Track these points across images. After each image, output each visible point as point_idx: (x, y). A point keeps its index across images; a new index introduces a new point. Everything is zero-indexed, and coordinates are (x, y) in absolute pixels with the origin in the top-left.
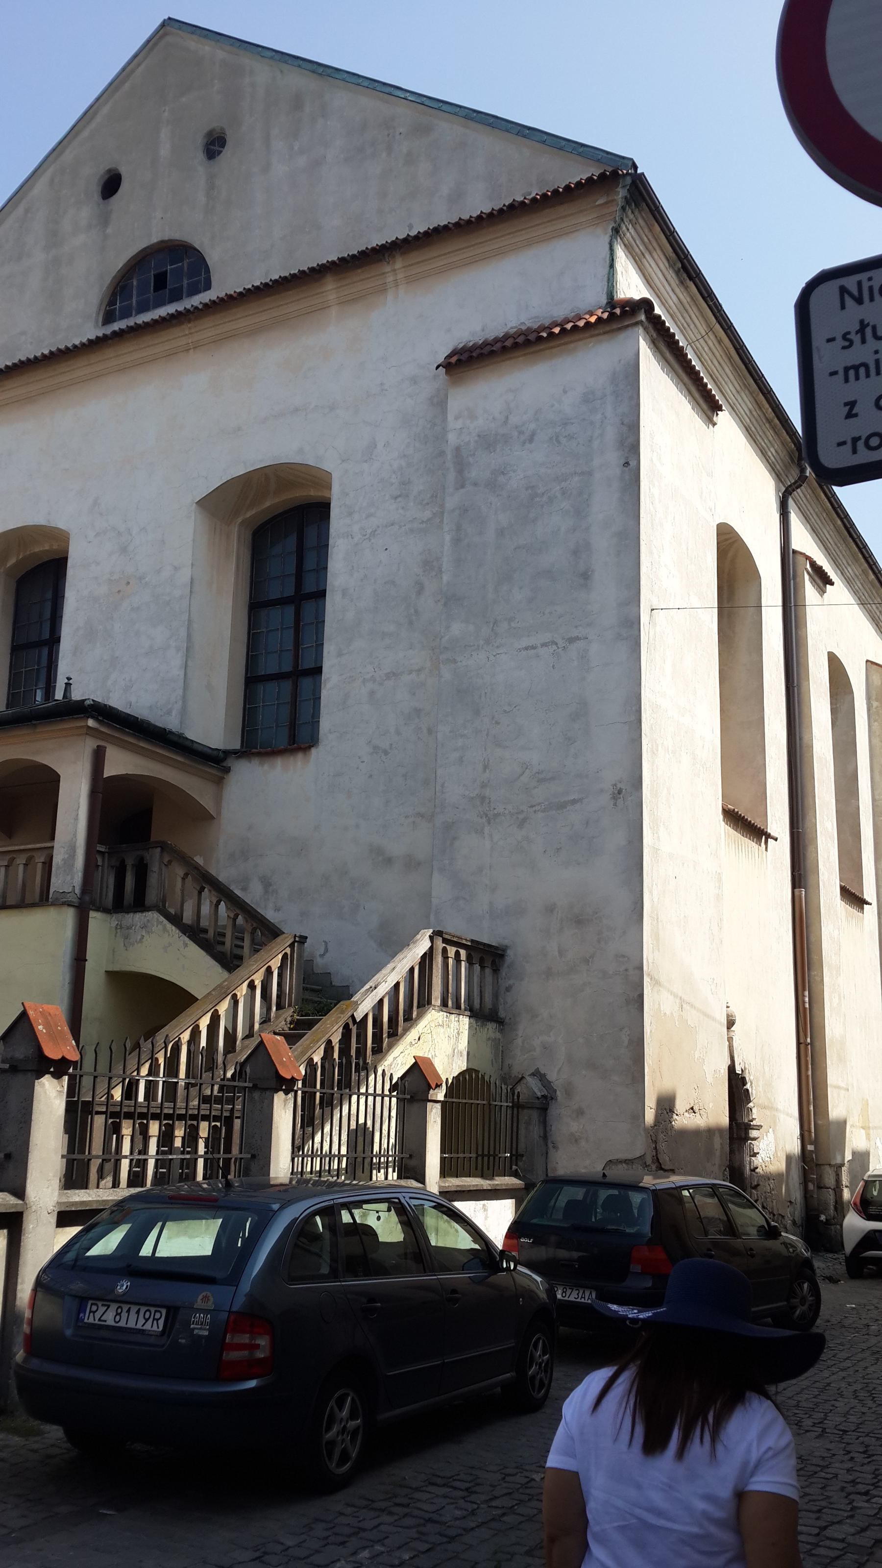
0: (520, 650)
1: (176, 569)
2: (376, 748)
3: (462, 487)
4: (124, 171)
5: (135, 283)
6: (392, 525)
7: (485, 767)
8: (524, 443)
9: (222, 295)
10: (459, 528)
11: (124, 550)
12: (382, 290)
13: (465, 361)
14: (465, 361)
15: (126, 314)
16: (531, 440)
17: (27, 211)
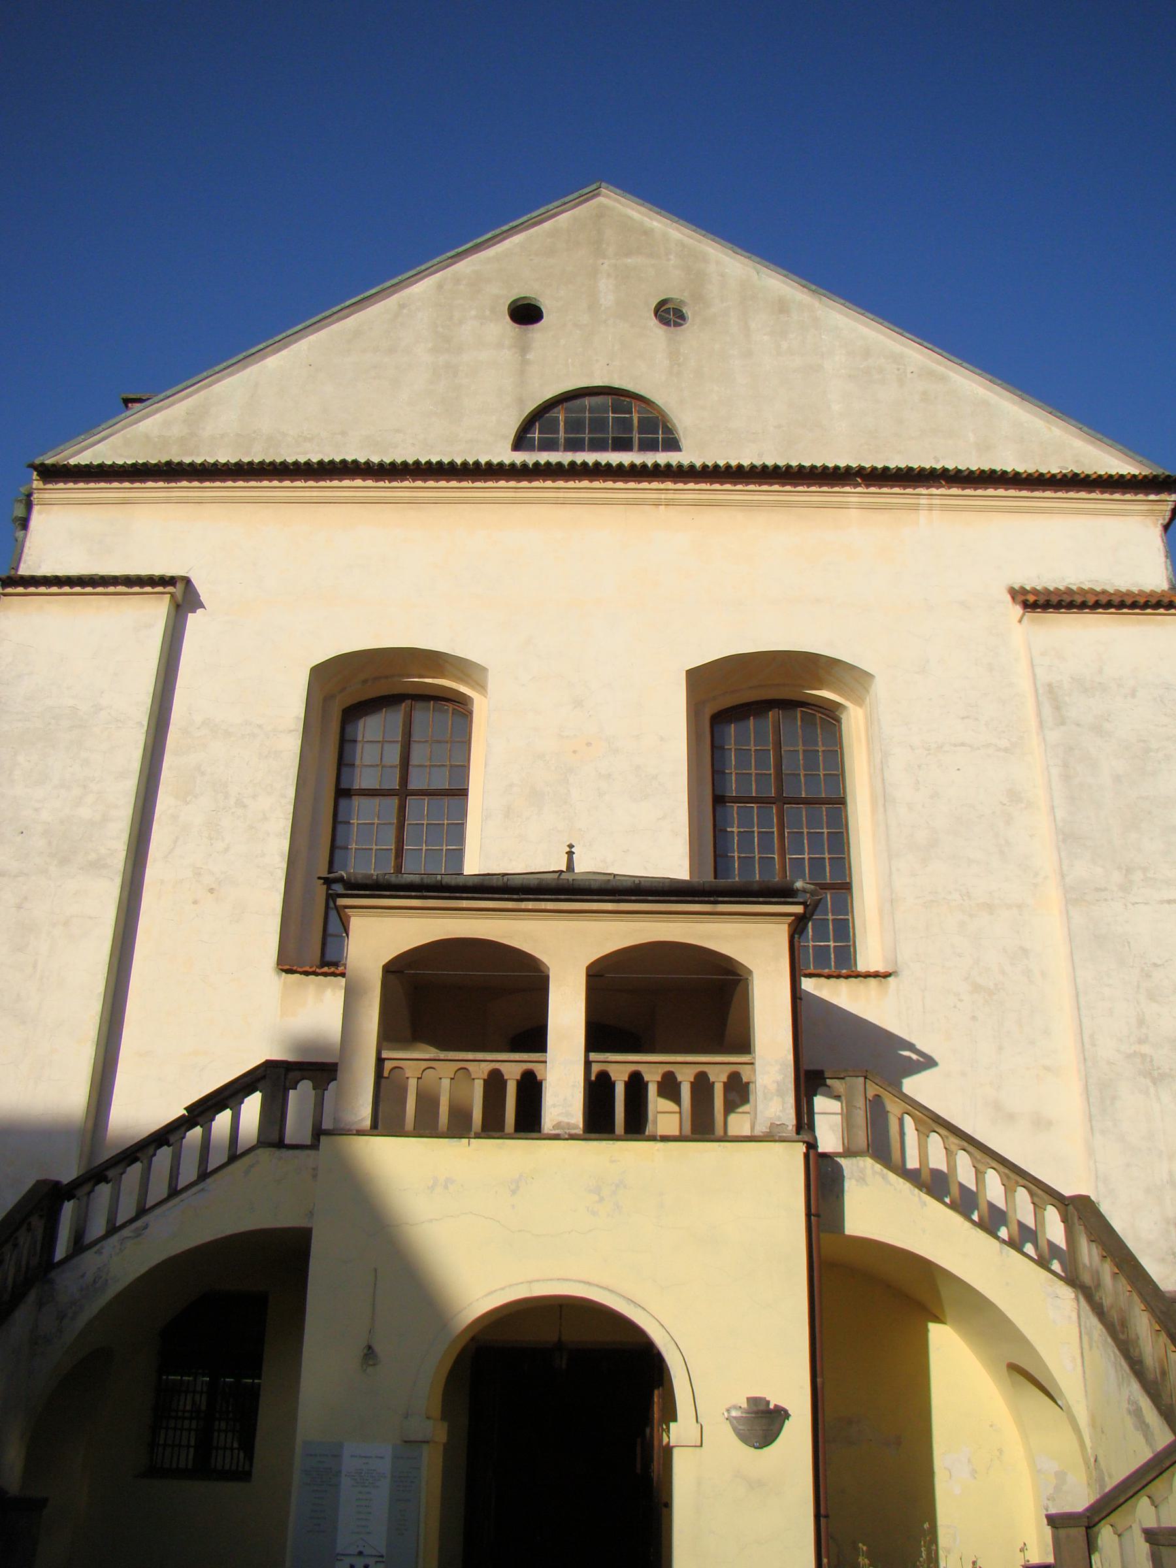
0: (1162, 902)
1: (662, 739)
2: (976, 988)
3: (1063, 723)
4: (546, 305)
5: (561, 417)
6: (963, 744)
7: (1141, 1022)
8: (1126, 697)
9: (686, 463)
10: (1066, 765)
11: (578, 703)
12: (916, 508)
13: (1039, 602)
14: (1039, 602)
15: (548, 445)
16: (1133, 694)
17: (402, 306)
